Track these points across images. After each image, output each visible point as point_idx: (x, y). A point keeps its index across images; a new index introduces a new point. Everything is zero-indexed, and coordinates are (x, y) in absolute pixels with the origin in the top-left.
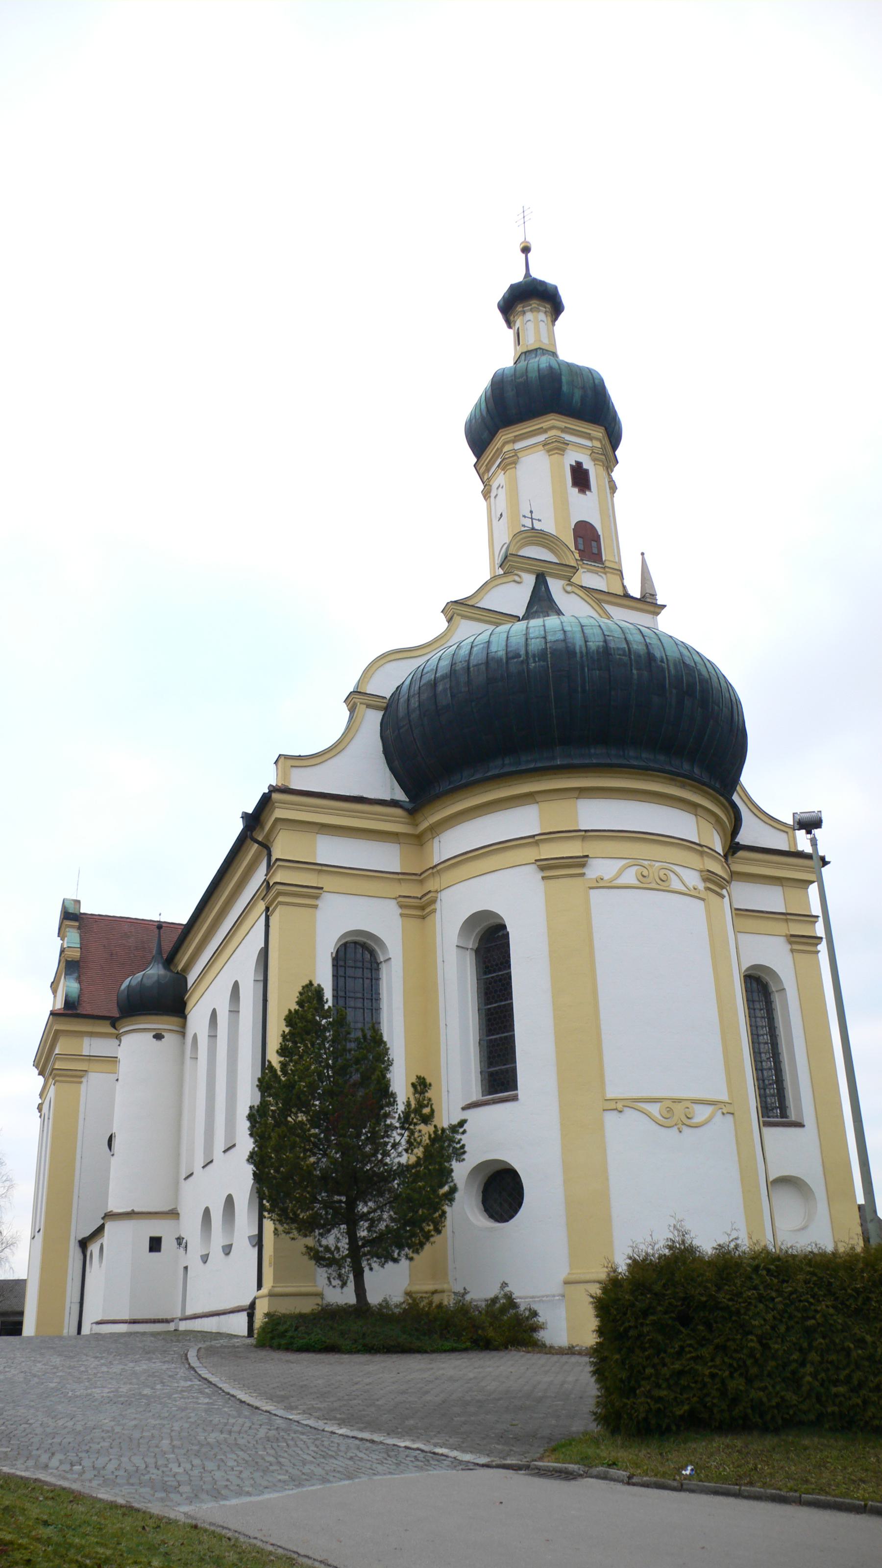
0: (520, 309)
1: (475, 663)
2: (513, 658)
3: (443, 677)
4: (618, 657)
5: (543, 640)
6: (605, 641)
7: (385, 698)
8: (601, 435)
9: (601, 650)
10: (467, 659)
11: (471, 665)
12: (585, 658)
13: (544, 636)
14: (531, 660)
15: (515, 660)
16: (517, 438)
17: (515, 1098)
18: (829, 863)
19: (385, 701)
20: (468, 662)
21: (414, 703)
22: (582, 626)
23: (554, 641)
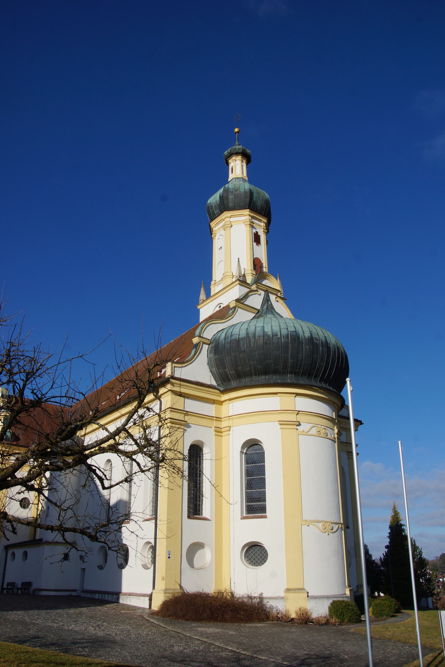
0: (234, 159)
1: (258, 335)
2: (275, 336)
3: (243, 339)
4: (315, 341)
5: (287, 330)
6: (311, 334)
7: (209, 340)
8: (266, 221)
9: (309, 337)
10: (254, 332)
11: (256, 335)
12: (303, 340)
13: (287, 328)
14: (282, 338)
15: (276, 337)
17: (265, 517)
18: (363, 424)
19: (210, 341)
20: (255, 334)
21: (228, 346)
22: (311, 332)
23: (291, 331)
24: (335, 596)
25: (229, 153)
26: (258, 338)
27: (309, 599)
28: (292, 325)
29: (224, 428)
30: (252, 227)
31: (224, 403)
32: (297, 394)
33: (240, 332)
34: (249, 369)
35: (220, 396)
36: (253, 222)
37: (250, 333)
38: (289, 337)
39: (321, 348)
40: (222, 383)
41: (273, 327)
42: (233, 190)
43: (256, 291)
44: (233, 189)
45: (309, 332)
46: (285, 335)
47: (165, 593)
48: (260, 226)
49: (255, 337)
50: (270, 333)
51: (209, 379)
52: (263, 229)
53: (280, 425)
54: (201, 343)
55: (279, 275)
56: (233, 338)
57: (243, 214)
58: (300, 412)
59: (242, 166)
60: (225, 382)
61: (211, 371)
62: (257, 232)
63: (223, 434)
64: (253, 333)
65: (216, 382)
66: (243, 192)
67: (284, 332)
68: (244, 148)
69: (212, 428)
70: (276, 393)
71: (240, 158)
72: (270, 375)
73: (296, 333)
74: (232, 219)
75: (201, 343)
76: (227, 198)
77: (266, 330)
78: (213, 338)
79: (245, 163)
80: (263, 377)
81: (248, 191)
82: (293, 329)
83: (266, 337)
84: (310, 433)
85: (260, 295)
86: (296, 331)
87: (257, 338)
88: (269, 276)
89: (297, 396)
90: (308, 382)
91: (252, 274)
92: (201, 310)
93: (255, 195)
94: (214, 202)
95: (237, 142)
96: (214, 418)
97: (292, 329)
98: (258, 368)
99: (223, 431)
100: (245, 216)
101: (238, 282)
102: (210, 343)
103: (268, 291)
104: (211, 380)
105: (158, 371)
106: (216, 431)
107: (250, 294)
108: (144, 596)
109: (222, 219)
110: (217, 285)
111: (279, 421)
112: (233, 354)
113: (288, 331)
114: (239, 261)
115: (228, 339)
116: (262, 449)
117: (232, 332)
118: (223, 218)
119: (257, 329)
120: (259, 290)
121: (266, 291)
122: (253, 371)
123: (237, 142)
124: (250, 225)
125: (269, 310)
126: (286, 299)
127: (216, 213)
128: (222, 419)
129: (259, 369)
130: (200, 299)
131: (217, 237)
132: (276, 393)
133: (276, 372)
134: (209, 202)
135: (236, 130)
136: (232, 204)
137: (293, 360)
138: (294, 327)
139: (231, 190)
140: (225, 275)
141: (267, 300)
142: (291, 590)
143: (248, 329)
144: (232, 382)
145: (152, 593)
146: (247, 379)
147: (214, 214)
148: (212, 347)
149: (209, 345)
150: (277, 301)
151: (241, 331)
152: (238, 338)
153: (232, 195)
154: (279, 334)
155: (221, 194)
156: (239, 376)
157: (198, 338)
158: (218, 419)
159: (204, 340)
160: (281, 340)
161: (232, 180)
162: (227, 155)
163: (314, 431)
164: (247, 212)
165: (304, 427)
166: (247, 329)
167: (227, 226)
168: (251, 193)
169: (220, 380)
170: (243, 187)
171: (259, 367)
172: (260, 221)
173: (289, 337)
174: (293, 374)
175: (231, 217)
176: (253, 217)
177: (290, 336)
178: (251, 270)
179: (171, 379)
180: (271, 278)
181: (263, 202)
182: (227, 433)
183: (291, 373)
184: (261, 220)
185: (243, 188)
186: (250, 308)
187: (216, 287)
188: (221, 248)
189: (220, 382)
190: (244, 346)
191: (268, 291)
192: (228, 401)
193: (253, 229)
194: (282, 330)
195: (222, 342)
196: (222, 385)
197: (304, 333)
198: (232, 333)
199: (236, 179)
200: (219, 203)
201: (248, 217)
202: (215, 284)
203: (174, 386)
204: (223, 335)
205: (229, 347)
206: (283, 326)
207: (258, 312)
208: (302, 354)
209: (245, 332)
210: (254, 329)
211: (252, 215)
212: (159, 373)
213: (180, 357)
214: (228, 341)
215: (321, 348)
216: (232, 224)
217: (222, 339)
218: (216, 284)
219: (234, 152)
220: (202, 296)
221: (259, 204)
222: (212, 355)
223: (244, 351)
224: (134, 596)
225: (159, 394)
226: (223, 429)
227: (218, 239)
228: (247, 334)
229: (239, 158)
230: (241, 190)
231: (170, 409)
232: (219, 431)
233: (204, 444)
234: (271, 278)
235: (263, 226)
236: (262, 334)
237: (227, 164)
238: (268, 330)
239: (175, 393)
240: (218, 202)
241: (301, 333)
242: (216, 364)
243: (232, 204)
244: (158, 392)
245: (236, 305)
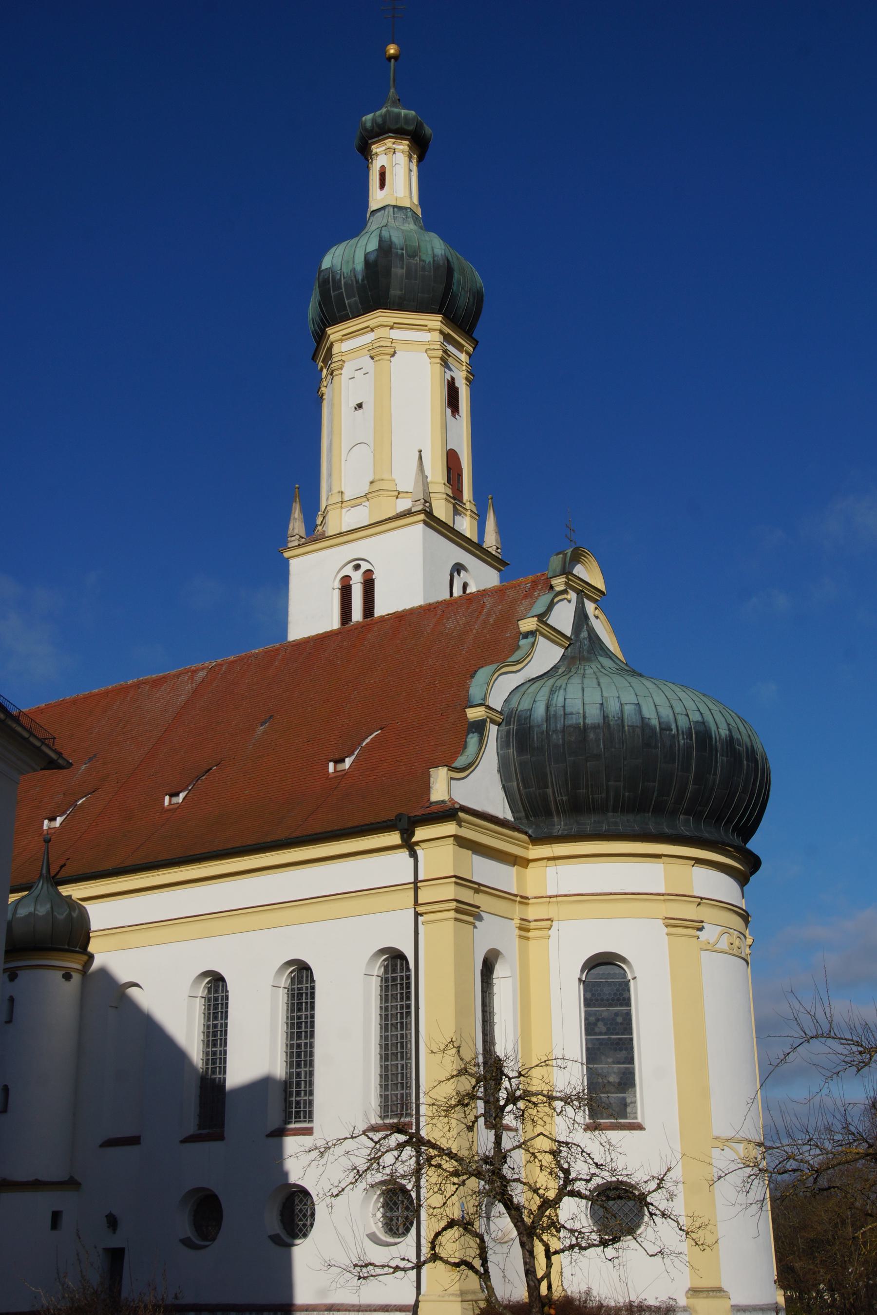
1: (630, 724)
3: (595, 727)
6: (730, 730)
8: (472, 349)
9: (728, 739)
10: (620, 715)
11: (626, 724)
12: (718, 743)
13: (685, 713)
14: (681, 737)
15: (668, 732)
16: (395, 325)
19: (502, 717)
20: (622, 719)
21: (557, 739)
24: (770, 1306)
25: (378, 126)
26: (631, 731)
27: (735, 1312)
28: (695, 708)
29: (536, 920)
30: (445, 364)
31: (531, 865)
33: (587, 711)
34: (604, 795)
35: (527, 848)
36: (445, 351)
37: (611, 718)
38: (694, 736)
39: (745, 762)
40: (527, 817)
41: (660, 709)
42: (404, 252)
43: (564, 592)
44: (402, 249)
46: (685, 730)
47: (462, 1302)
48: (459, 361)
49: (623, 727)
50: (655, 722)
51: (502, 809)
52: (467, 371)
53: (667, 926)
54: (488, 720)
55: (492, 499)
57: (426, 326)
58: (704, 901)
59: (411, 171)
60: (534, 816)
61: (504, 787)
62: (453, 379)
63: (531, 934)
64: (619, 718)
65: (512, 812)
66: (430, 262)
67: (683, 722)
68: (419, 119)
69: (513, 919)
71: (406, 148)
72: (646, 815)
73: (705, 726)
74: (395, 334)
75: (488, 720)
76: (388, 273)
78: (506, 710)
79: (415, 161)
81: (441, 263)
84: (719, 946)
85: (569, 601)
86: (703, 723)
87: (629, 729)
88: (589, 556)
89: (696, 865)
91: (447, 495)
92: (293, 563)
93: (456, 275)
94: (345, 270)
95: (392, 90)
96: (518, 899)
97: (695, 717)
98: (624, 796)
99: (531, 928)
100: (430, 330)
101: (422, 517)
102: (501, 720)
103: (584, 591)
104: (504, 808)
105: (331, 761)
106: (521, 928)
107: (556, 600)
108: (387, 1311)
109: (368, 327)
110: (346, 507)
111: (666, 918)
113: (690, 721)
114: (420, 457)
115: (556, 723)
117: (564, 707)
118: (371, 323)
120: (569, 590)
121: (579, 592)
122: (611, 802)
123: (392, 90)
124: (442, 359)
125: (594, 642)
126: (508, 564)
127: (348, 303)
128: (530, 901)
129: (626, 799)
130: (290, 532)
131: (347, 371)
133: (659, 810)
134: (326, 263)
135: (392, 50)
136: (400, 292)
137: (697, 787)
138: (698, 713)
139: (400, 252)
140: (376, 487)
141: (581, 617)
142: (701, 1291)
143: (605, 705)
144: (556, 819)
145: (417, 1301)
147: (342, 306)
148: (508, 732)
149: (499, 725)
150: (597, 617)
151: (587, 707)
152: (582, 723)
153: (402, 268)
154: (673, 727)
155: (372, 258)
157: (484, 709)
158: (524, 900)
159: (494, 714)
160: (679, 742)
161: (383, 208)
162: (372, 130)
163: (724, 944)
164: (435, 321)
165: (710, 933)
166: (602, 704)
167: (383, 350)
168: (450, 271)
169: (525, 810)
170: (429, 247)
171: (627, 794)
172: (460, 347)
173: (694, 736)
174: (690, 816)
175: (392, 328)
176: (447, 338)
177: (696, 733)
178: (444, 484)
179: (459, 813)
180: (590, 561)
181: (471, 297)
182: (545, 932)
183: (687, 813)
184: (463, 346)
185: (430, 252)
186: (555, 635)
187: (344, 511)
188: (360, 406)
189: (523, 814)
190: (598, 746)
191: (584, 592)
192: (546, 860)
193: (446, 370)
194: (679, 718)
195: (539, 726)
196: (525, 821)
197: (718, 728)
198: (566, 708)
199: (396, 209)
200: (363, 280)
201: (437, 337)
202: (342, 502)
203: (460, 826)
204: (540, 711)
205: (561, 741)
207: (569, 645)
208: (715, 774)
209: (598, 711)
210: (618, 708)
211: (447, 330)
212: (331, 765)
213: (381, 729)
214: (556, 726)
215: (745, 762)
216: (398, 347)
217: (539, 719)
218: (344, 505)
219: (394, 127)
220: (297, 526)
221: (464, 300)
222: (512, 751)
224: (346, 1310)
225: (414, 839)
226: (532, 924)
227: (350, 379)
228: (605, 717)
229: (403, 145)
230: (424, 257)
231: (453, 879)
233: (500, 956)
234: (590, 561)
235: (465, 364)
236: (639, 723)
237: (365, 153)
238: (648, 712)
239: (461, 842)
240: (360, 278)
241: (713, 728)
242: (522, 773)
243: (398, 293)
244: (412, 834)
245: (536, 628)
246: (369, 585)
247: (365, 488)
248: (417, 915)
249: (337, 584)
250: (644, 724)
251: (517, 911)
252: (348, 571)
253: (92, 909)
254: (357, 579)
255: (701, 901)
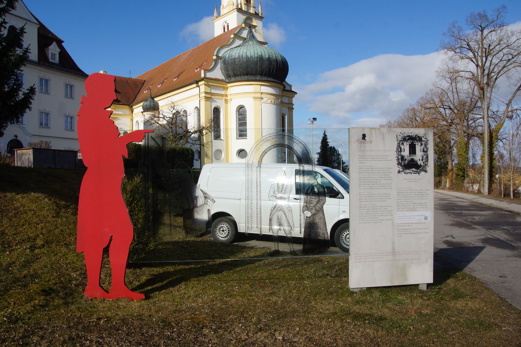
3: (237, 58)
6: (269, 56)
17: (247, 139)
21: (230, 61)
32: (261, 85)
41: (251, 53)
45: (268, 55)
50: (249, 56)
56: (233, 57)
67: (256, 55)
70: (252, 84)
77: (248, 54)
80: (246, 77)
82: (260, 54)
83: (247, 58)
84: (267, 102)
90: (267, 79)
97: (260, 54)
112: (232, 65)
116: (246, 109)
119: (244, 53)
132: (252, 84)
133: (251, 74)
140: (229, 3)
146: (239, 77)
154: (254, 57)
156: (235, 75)
163: (269, 101)
165: (265, 100)
204: (227, 56)
206: (256, 52)
208: (264, 66)
223: (237, 64)
228: (239, 56)
232: (226, 101)
238: (249, 54)
241: (264, 56)
246: (228, 26)
247: (227, 4)
248: (200, 100)
249: (223, 27)
250: (247, 57)
251: (224, 98)
252: (225, 24)
253: (159, 102)
254: (226, 25)
255: (262, 93)
